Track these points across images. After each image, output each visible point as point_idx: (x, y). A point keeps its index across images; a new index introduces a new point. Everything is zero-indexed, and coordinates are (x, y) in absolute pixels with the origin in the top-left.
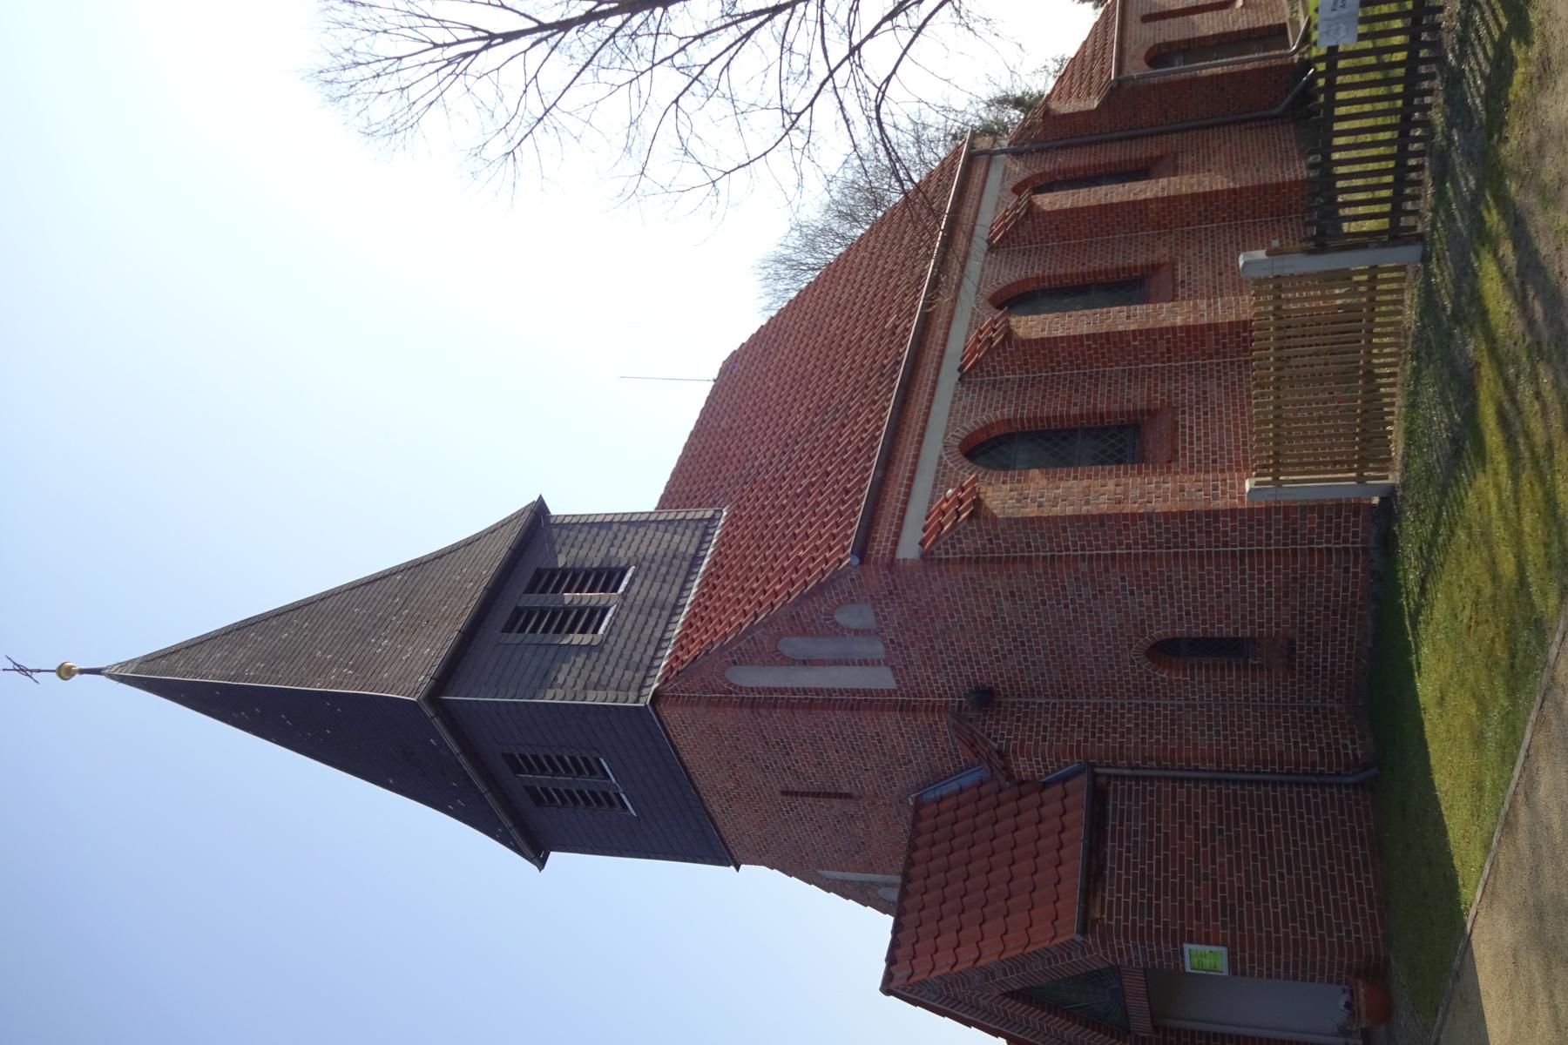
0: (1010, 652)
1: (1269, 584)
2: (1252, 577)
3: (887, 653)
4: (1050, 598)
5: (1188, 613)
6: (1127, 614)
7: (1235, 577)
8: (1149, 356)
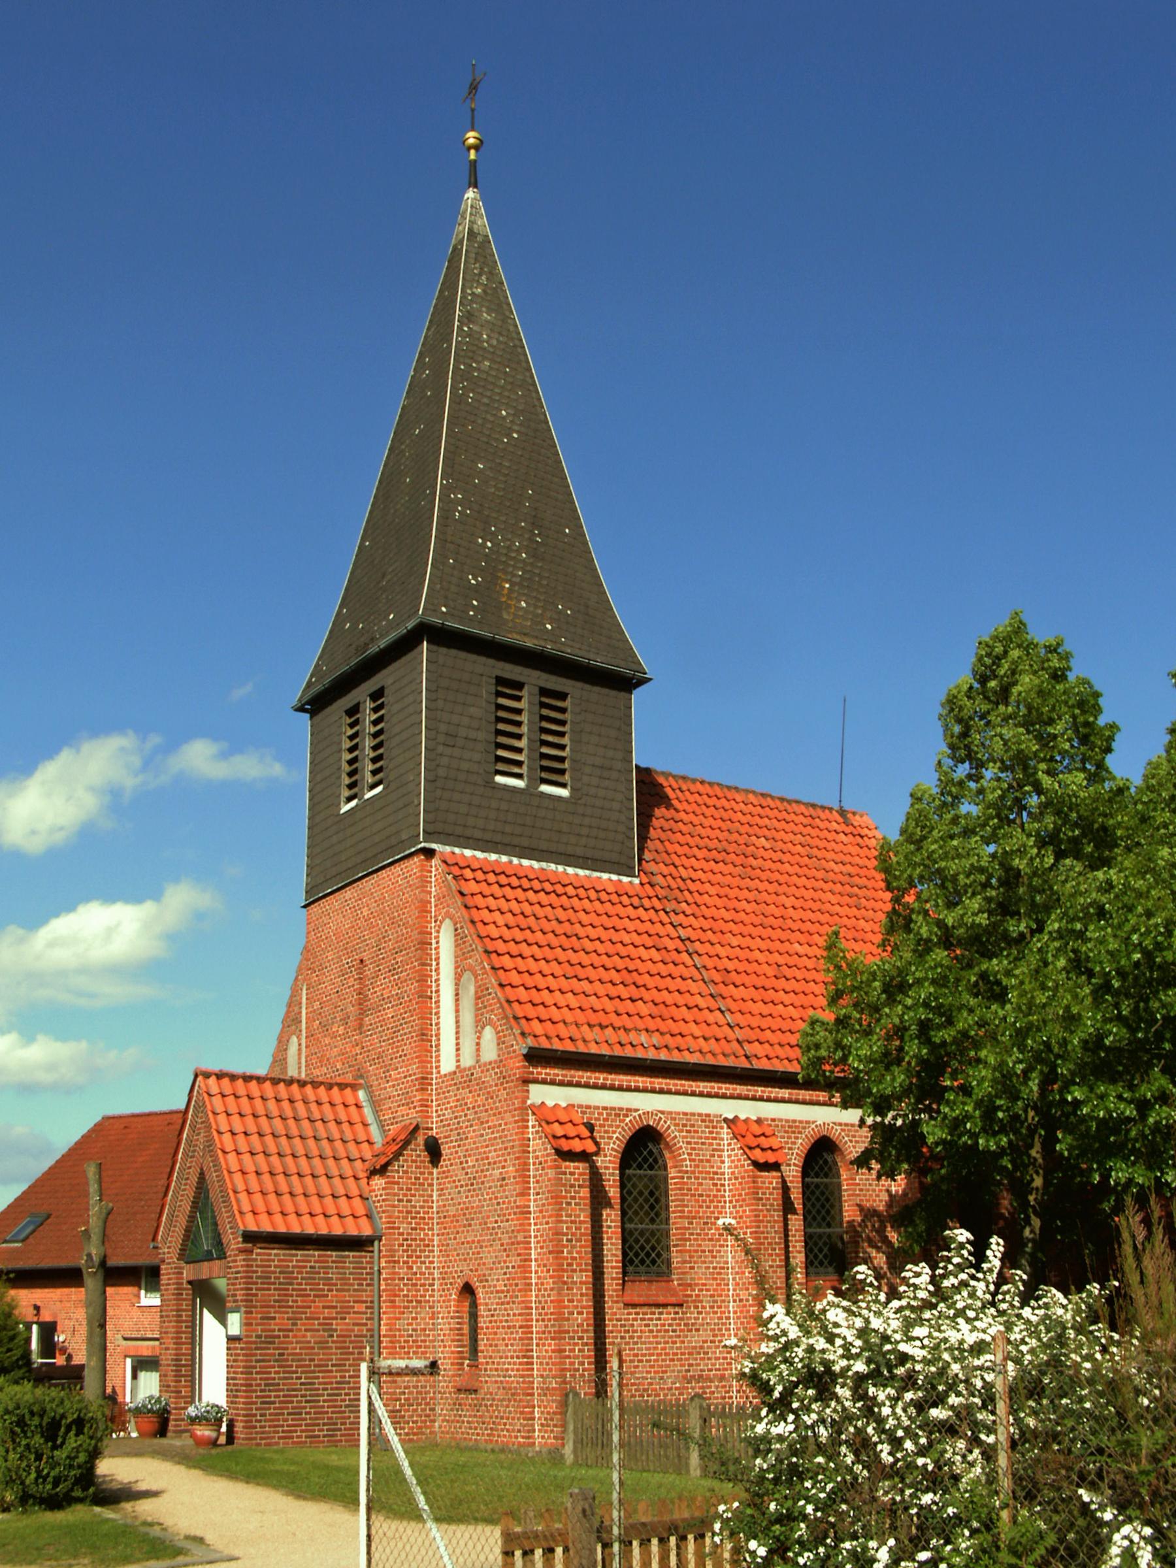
0: (467, 1174)
1: (510, 1376)
2: (515, 1363)
3: (465, 1069)
4: (502, 1209)
5: (493, 1315)
6: (492, 1269)
7: (515, 1351)
8: (737, 1284)
